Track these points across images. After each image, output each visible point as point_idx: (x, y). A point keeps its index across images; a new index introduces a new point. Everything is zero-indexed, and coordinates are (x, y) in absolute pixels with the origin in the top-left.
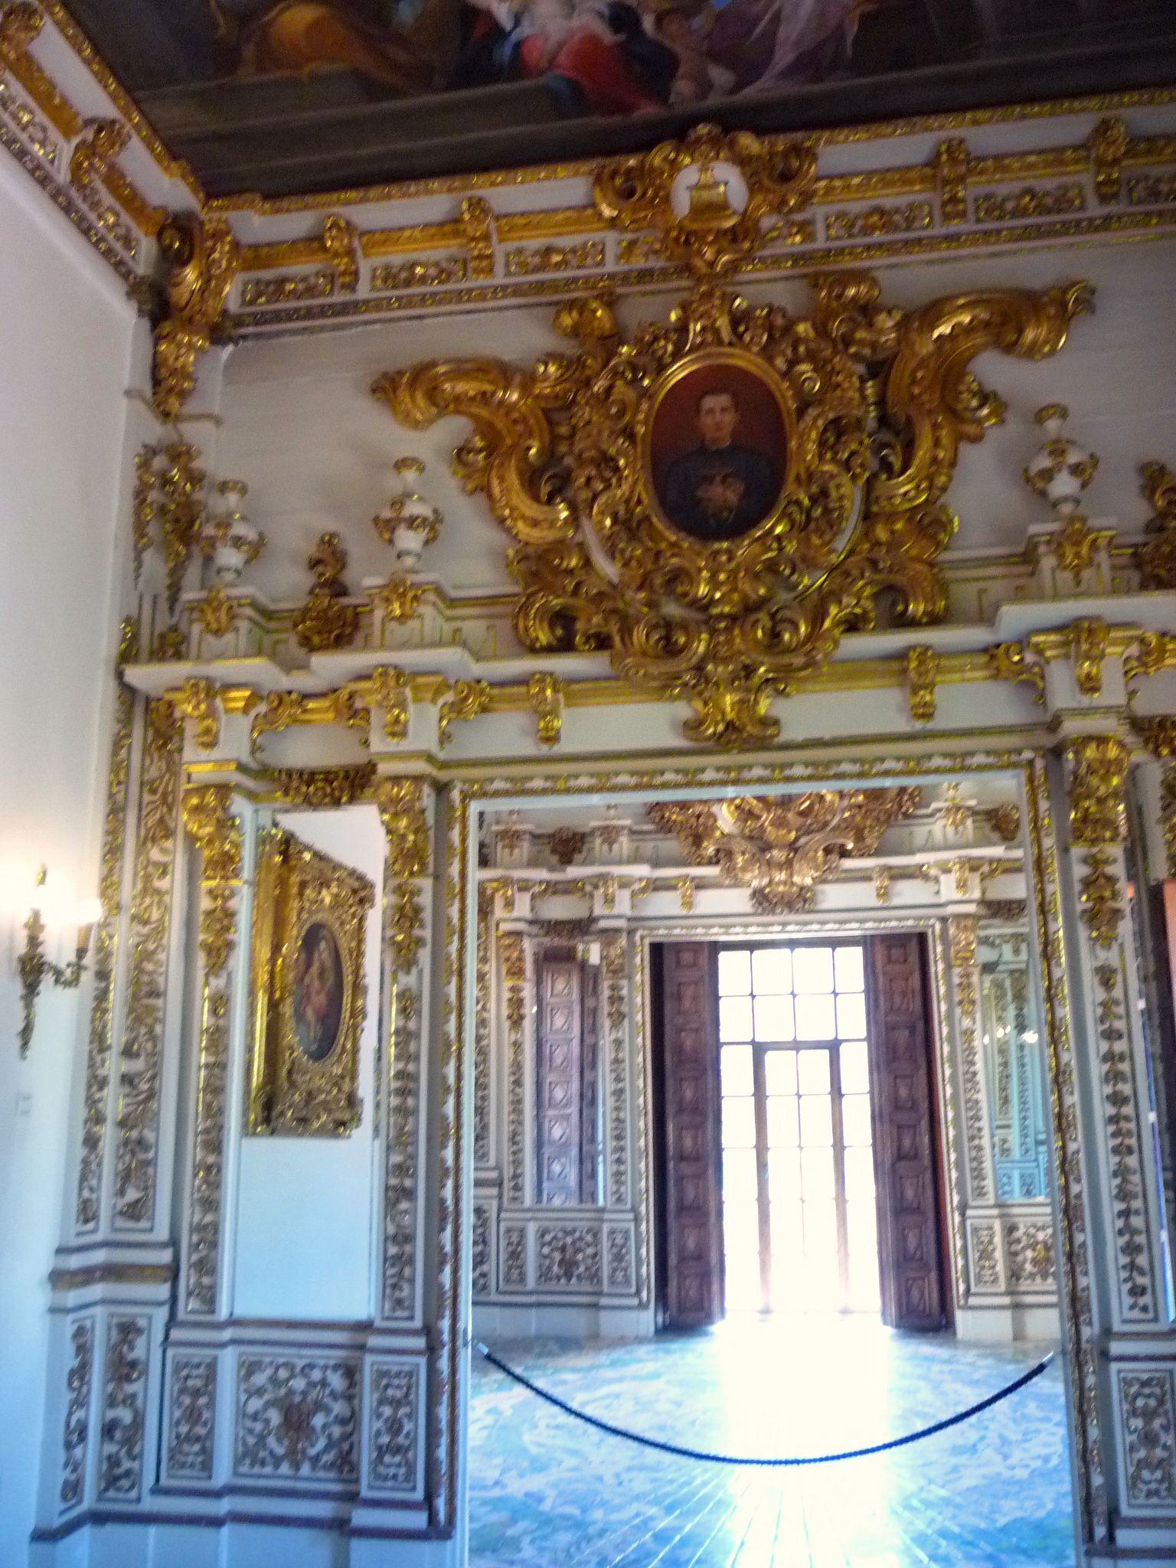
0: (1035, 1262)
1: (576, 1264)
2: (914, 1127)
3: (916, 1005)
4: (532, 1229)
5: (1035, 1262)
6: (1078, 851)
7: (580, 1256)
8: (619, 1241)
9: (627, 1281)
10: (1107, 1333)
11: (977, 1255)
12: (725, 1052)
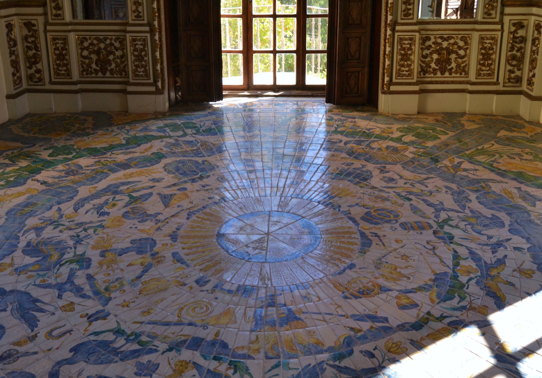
0: (438, 62)
1: (109, 62)
4: (72, 38)
5: (438, 62)
7: (111, 57)
8: (139, 47)
9: (147, 75)
11: (399, 57)
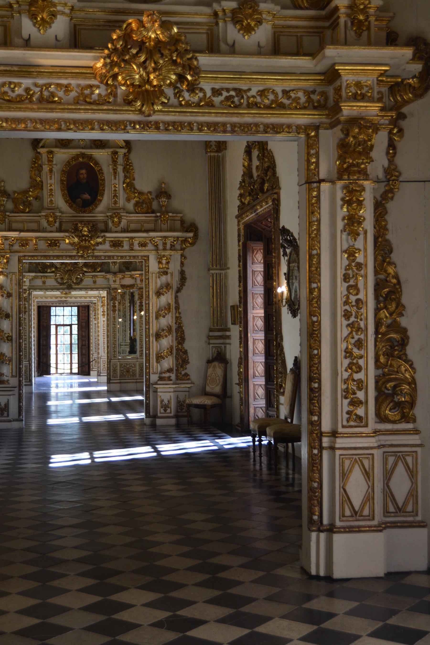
2: (85, 340)
3: (86, 318)
6: (102, 308)
10: (101, 356)
12: (52, 326)
